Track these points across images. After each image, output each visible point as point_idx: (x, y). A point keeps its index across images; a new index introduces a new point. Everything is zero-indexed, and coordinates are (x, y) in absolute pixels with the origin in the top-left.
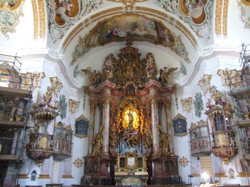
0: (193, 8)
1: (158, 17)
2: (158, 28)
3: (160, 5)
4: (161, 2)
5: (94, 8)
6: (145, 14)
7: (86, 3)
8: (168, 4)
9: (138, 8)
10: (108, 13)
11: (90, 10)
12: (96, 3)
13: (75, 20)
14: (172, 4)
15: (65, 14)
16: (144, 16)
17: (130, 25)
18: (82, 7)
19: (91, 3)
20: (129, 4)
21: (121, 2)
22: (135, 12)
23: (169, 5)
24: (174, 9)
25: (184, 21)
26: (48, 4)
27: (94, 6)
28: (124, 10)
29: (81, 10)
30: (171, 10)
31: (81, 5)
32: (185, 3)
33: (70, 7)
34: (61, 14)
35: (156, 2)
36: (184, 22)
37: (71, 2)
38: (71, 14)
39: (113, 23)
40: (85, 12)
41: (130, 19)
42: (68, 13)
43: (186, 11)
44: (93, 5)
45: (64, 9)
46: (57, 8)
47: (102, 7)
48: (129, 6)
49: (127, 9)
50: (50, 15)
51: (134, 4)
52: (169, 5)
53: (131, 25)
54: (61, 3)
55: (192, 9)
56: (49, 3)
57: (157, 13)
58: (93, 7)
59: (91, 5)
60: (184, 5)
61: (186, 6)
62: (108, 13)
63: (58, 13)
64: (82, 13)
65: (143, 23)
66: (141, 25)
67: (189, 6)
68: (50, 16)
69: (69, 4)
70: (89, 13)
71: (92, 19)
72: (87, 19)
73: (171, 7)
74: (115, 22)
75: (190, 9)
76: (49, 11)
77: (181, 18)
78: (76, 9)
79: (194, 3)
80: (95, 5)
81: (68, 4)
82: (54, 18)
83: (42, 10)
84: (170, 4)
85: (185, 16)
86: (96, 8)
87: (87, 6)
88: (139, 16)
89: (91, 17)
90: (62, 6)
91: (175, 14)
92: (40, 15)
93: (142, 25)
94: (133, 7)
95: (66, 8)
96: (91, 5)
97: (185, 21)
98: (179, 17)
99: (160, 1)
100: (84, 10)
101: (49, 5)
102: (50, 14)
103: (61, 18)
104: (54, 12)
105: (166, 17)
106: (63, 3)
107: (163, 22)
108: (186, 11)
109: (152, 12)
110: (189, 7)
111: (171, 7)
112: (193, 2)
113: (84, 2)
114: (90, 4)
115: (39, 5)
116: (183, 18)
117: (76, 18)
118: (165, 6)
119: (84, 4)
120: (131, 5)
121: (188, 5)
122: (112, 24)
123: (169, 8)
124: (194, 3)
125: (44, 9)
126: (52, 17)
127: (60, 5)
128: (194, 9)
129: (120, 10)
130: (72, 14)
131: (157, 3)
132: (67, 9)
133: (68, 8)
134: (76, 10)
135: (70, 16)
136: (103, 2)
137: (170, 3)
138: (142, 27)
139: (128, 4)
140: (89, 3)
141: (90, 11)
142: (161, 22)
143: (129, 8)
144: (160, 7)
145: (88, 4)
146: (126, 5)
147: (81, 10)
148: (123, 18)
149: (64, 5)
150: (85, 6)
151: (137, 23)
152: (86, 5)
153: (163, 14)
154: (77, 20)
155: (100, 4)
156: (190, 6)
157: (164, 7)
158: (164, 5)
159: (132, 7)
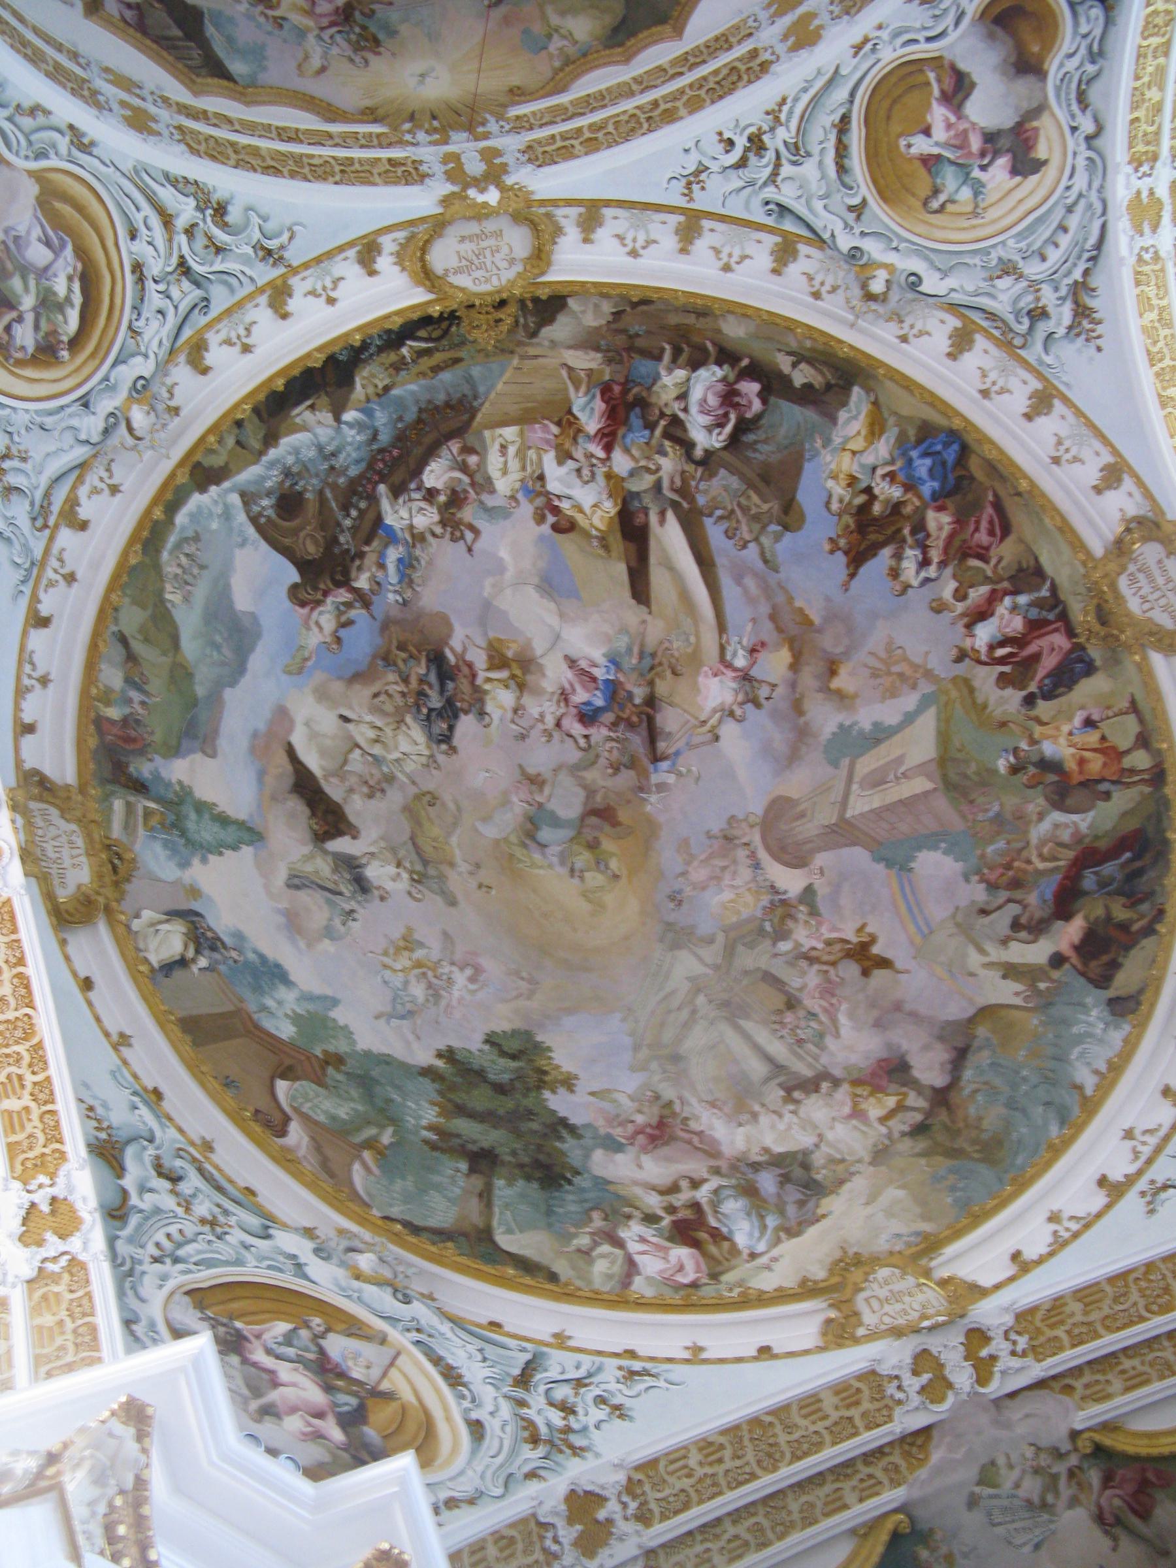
0: (17, 239)
1: (230, 121)
2: (180, 26)
3: (255, 220)
4: (250, 251)
5: (741, 142)
6: (330, 136)
7: (809, 169)
8: (200, 241)
9: (411, 174)
10: (628, 105)
11: (777, 119)
12: (732, 173)
13: (896, 34)
14: (170, 240)
15: (975, 77)
16: (331, 113)
17: (404, 29)
18: (839, 141)
19: (769, 170)
20: (480, 198)
21: (543, 203)
22: (408, 137)
23: (190, 232)
24: (147, 209)
25: (54, 120)
26: (1097, 143)
27: (747, 150)
28: (510, 144)
29: (845, 119)
30: (166, 195)
31: (842, 150)
32: (79, 266)
33: (927, 132)
34: (1004, 73)
35: (286, 236)
36: (47, 113)
37: (922, 172)
38: (928, 84)
39: (549, 37)
40: (815, 101)
41: (422, 76)
42: (948, 84)
43: (59, 205)
44: (753, 159)
45: (974, 118)
46: (1031, 120)
47: (686, 151)
48: (481, 183)
49: (489, 155)
50: (1093, 62)
51: (446, 201)
52: (190, 232)
53: (393, 33)
54: (996, 154)
55: (22, 230)
56: (1090, 148)
57: (255, 152)
58: (756, 144)
59: (770, 155)
60: (82, 253)
61: (69, 251)
62: (628, 105)
63: (1024, 86)
64: (841, 94)
65: (307, 57)
66: (319, 37)
67: (48, 255)
68: (1096, 55)
69: (938, 157)
70: (784, 101)
71: (754, 53)
72: (803, 53)
73: (167, 220)
74: (538, 45)
75: (37, 232)
76: (1094, 94)
77: (81, 143)
78: (889, 118)
79: (16, 283)
80: (742, 163)
81: (946, 154)
82: (1067, 41)
83: (1148, 95)
84: (183, 239)
85: (53, 162)
86: (731, 143)
87: (797, 150)
88: (370, 114)
89: (765, 67)
90: (990, 136)
91: (127, 167)
92: (1162, 60)
93: (311, 39)
94: (450, 176)
95: (963, 126)
96: (770, 155)
97: (41, 120)
98: (92, 144)
99: (263, 248)
100: (827, 119)
101: (1089, 139)
102: (1091, 69)
103: (1010, 42)
104: (1058, 90)
105: (179, 128)
106: (983, 154)
107: (178, 92)
108: (59, 205)
109: (298, 159)
110: (48, 244)
111: (167, 220)
112: (26, 289)
113: (824, 177)
114: (778, 165)
115: (1158, 133)
116: (63, 143)
117: (889, 55)
118: (213, 216)
119: (821, 163)
120: (472, 193)
121: (57, 252)
122: (555, 20)
123: (186, 210)
124: (16, 283)
125: (1135, 106)
126: (1083, 51)
127: (1004, 143)
128: (6, 231)
129: (539, 142)
130: (920, 79)
131: (279, 235)
132: (953, 119)
133: (949, 126)
134: (882, 113)
135: (936, 62)
136: (679, 186)
137: (186, 250)
138: (297, 19)
139: (492, 196)
140: (786, 170)
141: (774, 115)
142: (190, 85)
143: (475, 166)
144: (250, 208)
145: (795, 163)
146: (502, 188)
147: (845, 119)
148: (493, 83)
149: (975, 143)
150: (815, 149)
151: (357, 48)
152: (809, 154)
153: (216, 152)
154: (885, 35)
155: (701, 169)
156: (38, 254)
157: (220, 210)
158: (225, 226)
159: (455, 171)
